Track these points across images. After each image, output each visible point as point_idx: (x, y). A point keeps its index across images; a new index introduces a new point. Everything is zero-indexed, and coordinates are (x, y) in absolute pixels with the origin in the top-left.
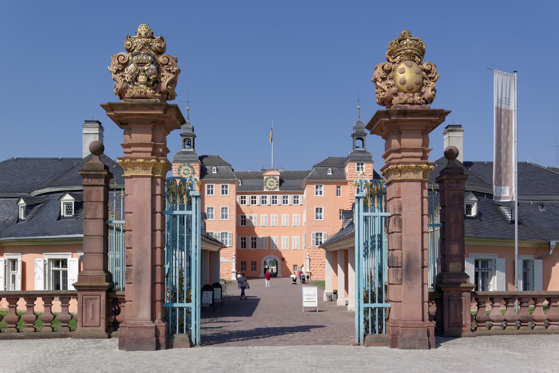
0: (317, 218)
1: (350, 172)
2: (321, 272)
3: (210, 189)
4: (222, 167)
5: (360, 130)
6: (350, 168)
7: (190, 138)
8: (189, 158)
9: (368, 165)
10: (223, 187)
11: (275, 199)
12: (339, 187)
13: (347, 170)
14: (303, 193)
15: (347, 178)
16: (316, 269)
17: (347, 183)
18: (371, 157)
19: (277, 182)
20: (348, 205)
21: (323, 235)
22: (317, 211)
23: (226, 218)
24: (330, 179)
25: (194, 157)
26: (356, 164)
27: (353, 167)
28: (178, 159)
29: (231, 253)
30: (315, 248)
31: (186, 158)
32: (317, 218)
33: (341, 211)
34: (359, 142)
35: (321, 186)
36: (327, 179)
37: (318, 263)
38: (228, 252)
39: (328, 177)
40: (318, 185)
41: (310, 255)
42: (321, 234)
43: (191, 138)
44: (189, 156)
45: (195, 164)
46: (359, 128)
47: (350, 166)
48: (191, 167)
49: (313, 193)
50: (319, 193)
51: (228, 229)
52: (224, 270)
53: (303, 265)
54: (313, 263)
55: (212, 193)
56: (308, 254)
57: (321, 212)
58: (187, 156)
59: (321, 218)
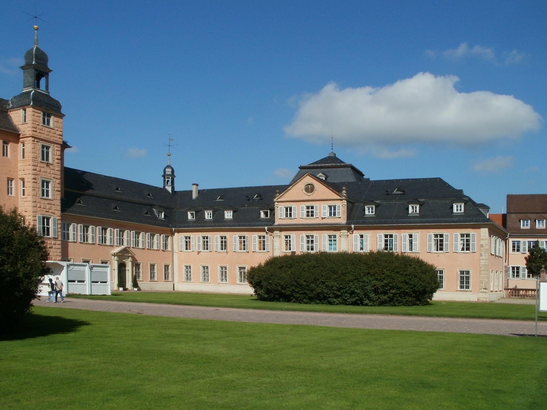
1: (34, 122)
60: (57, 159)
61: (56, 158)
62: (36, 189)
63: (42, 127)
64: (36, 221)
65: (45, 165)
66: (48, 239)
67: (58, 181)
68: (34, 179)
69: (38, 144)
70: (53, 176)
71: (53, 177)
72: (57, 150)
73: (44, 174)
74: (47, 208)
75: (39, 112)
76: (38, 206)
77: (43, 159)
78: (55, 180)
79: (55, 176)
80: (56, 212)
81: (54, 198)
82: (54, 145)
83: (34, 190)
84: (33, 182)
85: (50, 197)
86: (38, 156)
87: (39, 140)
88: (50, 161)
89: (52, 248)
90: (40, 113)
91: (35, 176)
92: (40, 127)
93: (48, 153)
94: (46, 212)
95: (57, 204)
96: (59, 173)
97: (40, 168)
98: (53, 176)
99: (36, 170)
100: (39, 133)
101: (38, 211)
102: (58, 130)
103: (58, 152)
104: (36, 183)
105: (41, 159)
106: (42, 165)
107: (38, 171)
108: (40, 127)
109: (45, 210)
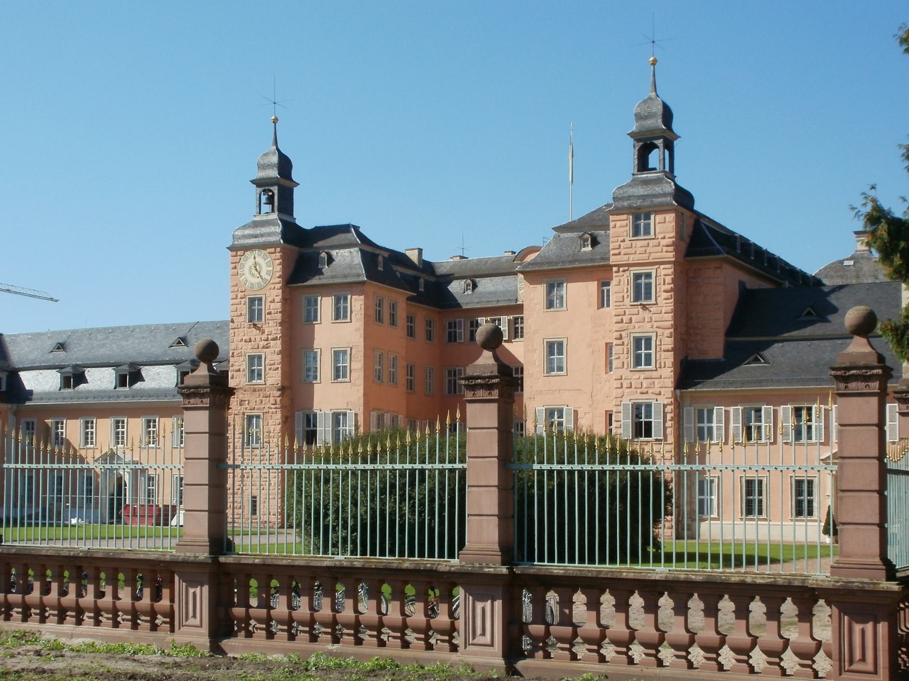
1: (616, 239)
7: (271, 188)
9: (659, 218)
22: (551, 352)
58: (259, 232)
60: (666, 291)
61: (664, 288)
62: (622, 356)
69: (625, 276)
70: (655, 324)
71: (657, 327)
72: (665, 275)
73: (637, 325)
74: (644, 385)
75: (625, 217)
76: (625, 386)
77: (637, 297)
78: (660, 331)
79: (659, 324)
80: (663, 391)
82: (659, 268)
83: (619, 358)
86: (625, 297)
87: (626, 268)
90: (626, 218)
91: (619, 333)
93: (648, 286)
94: (642, 393)
96: (670, 316)
97: (630, 316)
98: (655, 324)
99: (622, 321)
101: (625, 394)
102: (664, 238)
103: (667, 277)
104: (623, 344)
105: (632, 300)
106: (635, 310)
107: (626, 323)
108: (628, 243)
109: (639, 391)
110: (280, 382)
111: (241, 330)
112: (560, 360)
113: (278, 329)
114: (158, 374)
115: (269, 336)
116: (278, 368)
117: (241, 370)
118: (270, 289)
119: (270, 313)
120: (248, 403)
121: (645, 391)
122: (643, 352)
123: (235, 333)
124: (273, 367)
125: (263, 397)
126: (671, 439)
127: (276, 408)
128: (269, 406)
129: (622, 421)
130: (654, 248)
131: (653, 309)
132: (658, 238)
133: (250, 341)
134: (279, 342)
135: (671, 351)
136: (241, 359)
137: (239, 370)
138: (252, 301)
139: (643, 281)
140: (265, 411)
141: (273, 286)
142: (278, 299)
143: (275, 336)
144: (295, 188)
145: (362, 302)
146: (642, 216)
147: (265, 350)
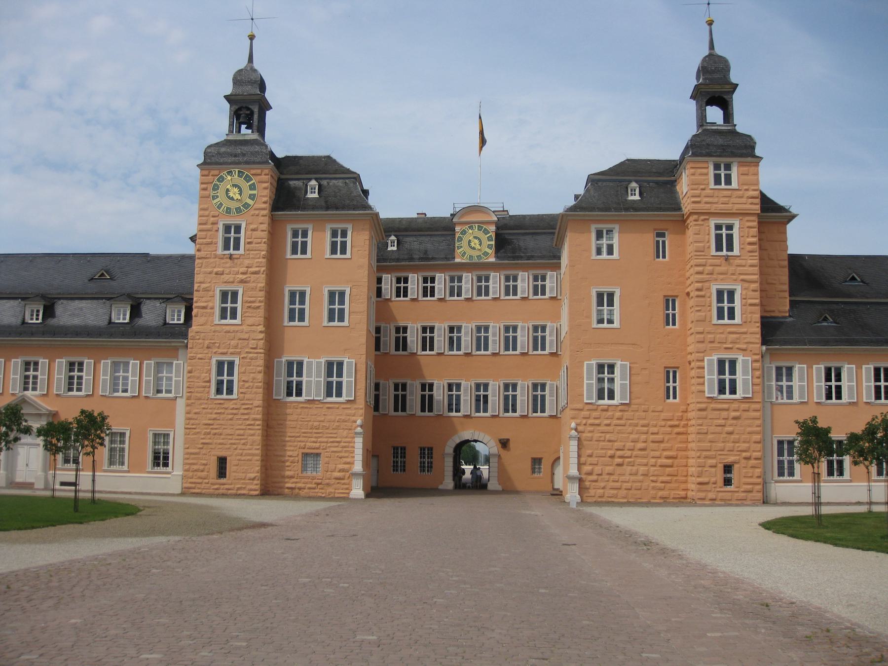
0: (600, 321)
1: (696, 187)
2: (612, 477)
3: (300, 239)
4: (334, 181)
5: (716, 76)
6: (693, 177)
7: (250, 107)
8: (244, 155)
10: (334, 234)
11: (483, 284)
12: (662, 235)
13: (684, 186)
14: (557, 267)
15: (683, 209)
16: (598, 470)
17: (684, 221)
18: (753, 148)
19: (489, 239)
20: (689, 282)
21: (617, 370)
22: (600, 303)
23: (341, 319)
24: (636, 210)
25: (257, 152)
26: (711, 167)
27: (700, 174)
28: (213, 159)
29: (354, 418)
30: (595, 407)
31: (235, 156)
32: (600, 321)
33: (667, 301)
34: (714, 114)
35: (609, 231)
36: (627, 210)
37: (604, 451)
38: (343, 417)
39: (633, 207)
40: (600, 226)
41: (580, 428)
42: (611, 367)
43: (256, 110)
44: (245, 149)
45: (259, 171)
46: (713, 72)
47: (692, 170)
48: (248, 179)
49: (589, 250)
50: (605, 250)
51: (346, 350)
52: (331, 466)
53: (559, 458)
54: (589, 452)
55: (304, 252)
56: (573, 425)
57: (611, 303)
58: (239, 151)
59: (610, 321)
60: (750, 244)
63: (712, 191)
64: (704, 368)
65: (723, 261)
66: (732, 401)
67: (756, 286)
68: (698, 290)
77: (719, 248)
78: (746, 285)
81: (744, 320)
84: (698, 296)
85: (738, 320)
87: (707, 217)
88: (736, 251)
89: (740, 419)
92: (708, 192)
93: (730, 238)
95: (751, 331)
96: (756, 270)
100: (706, 203)
106: (717, 261)
107: (708, 274)
110: (262, 323)
111: (212, 260)
112: (611, 313)
113: (261, 262)
114: (81, 309)
115: (250, 270)
116: (258, 307)
117: (209, 307)
118: (252, 216)
119: (249, 243)
120: (219, 347)
121: (730, 346)
122: (726, 305)
123: (202, 263)
124: (253, 305)
125: (240, 339)
126: (758, 399)
127: (257, 353)
128: (247, 350)
129: (706, 377)
130: (737, 199)
131: (738, 261)
132: (741, 190)
133: (222, 274)
134: (262, 277)
135: (758, 305)
136: (211, 293)
137: (204, 308)
138: (227, 229)
139: (724, 232)
140: (242, 356)
141: (257, 212)
142: (265, 227)
143: (257, 269)
144: (267, 112)
145: (367, 237)
146: (722, 166)
147: (242, 285)
